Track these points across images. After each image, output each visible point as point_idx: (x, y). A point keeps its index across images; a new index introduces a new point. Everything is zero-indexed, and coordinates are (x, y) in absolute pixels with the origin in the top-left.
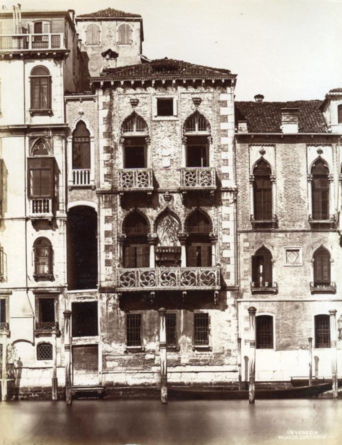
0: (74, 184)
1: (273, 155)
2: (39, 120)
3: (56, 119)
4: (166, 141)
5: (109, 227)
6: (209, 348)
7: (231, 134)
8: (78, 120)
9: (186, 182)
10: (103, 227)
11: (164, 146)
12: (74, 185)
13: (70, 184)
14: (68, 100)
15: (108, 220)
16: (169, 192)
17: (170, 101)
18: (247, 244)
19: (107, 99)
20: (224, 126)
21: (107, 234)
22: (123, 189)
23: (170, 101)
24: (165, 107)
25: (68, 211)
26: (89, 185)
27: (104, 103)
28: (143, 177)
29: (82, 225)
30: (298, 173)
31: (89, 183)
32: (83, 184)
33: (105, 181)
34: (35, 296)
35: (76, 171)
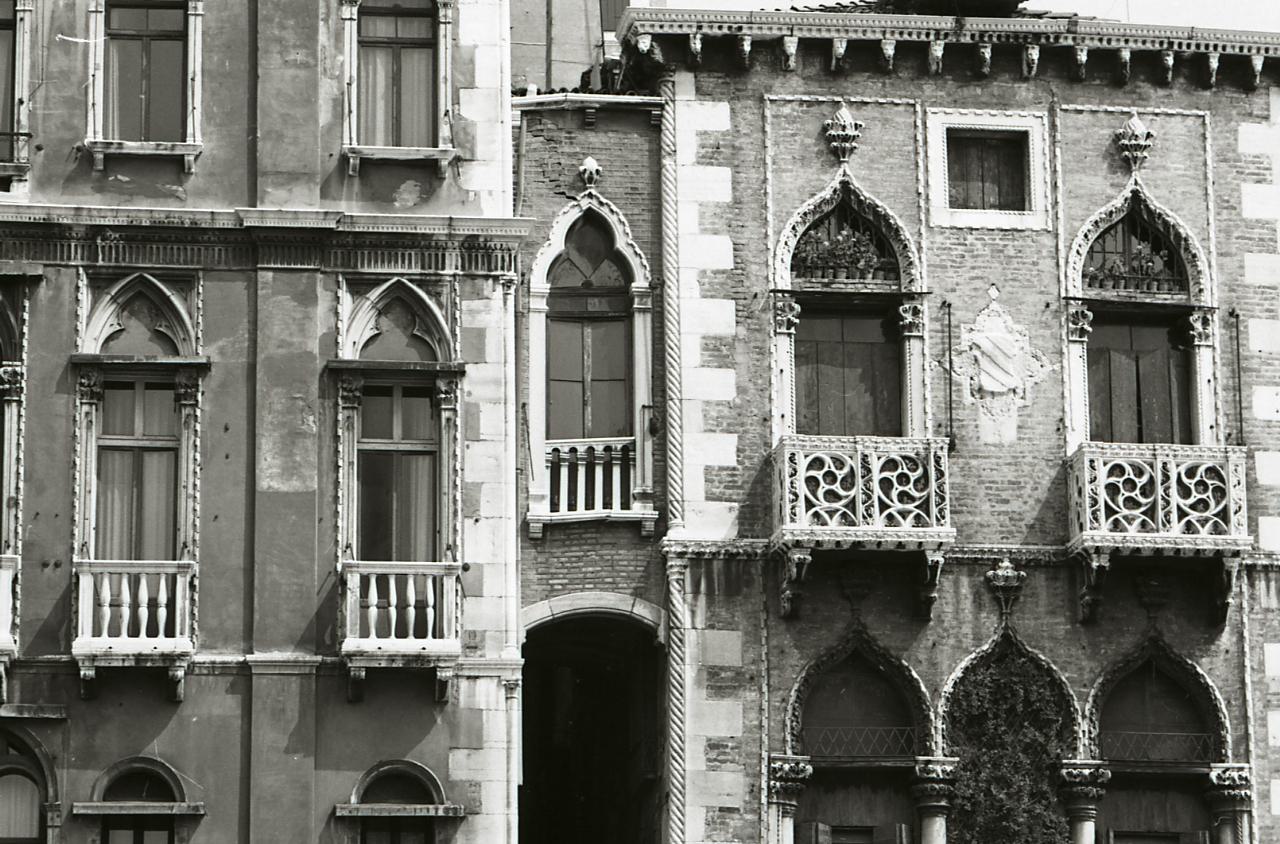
0: (555, 507)
9: (1110, 512)
10: (699, 719)
11: (986, 346)
12: (556, 517)
15: (719, 682)
16: (1017, 565)
17: (1015, 145)
22: (812, 532)
23: (1015, 145)
24: (993, 166)
26: (626, 514)
28: (903, 479)
31: (625, 505)
32: (599, 512)
33: (708, 499)
35: (564, 446)
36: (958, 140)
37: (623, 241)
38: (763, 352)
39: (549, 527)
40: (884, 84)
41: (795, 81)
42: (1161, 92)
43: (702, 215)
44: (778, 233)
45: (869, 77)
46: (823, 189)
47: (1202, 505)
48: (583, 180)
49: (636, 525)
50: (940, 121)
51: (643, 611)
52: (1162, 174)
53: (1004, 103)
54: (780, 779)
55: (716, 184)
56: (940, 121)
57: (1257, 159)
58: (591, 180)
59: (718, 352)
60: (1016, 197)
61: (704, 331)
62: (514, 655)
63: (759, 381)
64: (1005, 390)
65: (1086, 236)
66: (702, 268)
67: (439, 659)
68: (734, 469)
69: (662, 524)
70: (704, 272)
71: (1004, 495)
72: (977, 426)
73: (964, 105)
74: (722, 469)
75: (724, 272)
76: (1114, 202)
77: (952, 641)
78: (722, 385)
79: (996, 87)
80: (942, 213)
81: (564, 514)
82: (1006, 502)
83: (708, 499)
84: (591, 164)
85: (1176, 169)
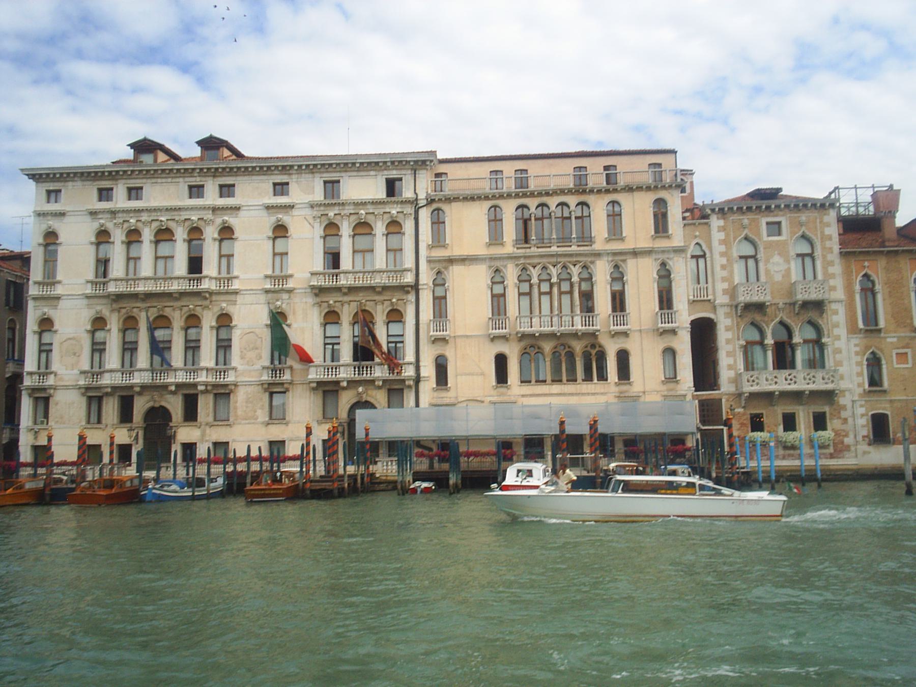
1: (879, 270)
2: (662, 244)
4: (776, 259)
5: (729, 335)
13: (691, 297)
15: (728, 329)
18: (858, 349)
19: (721, 223)
20: (828, 244)
21: (728, 341)
29: (703, 334)
36: (768, 223)
37: (704, 247)
38: (732, 267)
48: (696, 237)
49: (709, 300)
50: (764, 221)
51: (712, 316)
55: (722, 236)
59: (723, 267)
60: (780, 234)
69: (715, 300)
78: (724, 273)
79: (775, 213)
80: (765, 238)
84: (697, 233)
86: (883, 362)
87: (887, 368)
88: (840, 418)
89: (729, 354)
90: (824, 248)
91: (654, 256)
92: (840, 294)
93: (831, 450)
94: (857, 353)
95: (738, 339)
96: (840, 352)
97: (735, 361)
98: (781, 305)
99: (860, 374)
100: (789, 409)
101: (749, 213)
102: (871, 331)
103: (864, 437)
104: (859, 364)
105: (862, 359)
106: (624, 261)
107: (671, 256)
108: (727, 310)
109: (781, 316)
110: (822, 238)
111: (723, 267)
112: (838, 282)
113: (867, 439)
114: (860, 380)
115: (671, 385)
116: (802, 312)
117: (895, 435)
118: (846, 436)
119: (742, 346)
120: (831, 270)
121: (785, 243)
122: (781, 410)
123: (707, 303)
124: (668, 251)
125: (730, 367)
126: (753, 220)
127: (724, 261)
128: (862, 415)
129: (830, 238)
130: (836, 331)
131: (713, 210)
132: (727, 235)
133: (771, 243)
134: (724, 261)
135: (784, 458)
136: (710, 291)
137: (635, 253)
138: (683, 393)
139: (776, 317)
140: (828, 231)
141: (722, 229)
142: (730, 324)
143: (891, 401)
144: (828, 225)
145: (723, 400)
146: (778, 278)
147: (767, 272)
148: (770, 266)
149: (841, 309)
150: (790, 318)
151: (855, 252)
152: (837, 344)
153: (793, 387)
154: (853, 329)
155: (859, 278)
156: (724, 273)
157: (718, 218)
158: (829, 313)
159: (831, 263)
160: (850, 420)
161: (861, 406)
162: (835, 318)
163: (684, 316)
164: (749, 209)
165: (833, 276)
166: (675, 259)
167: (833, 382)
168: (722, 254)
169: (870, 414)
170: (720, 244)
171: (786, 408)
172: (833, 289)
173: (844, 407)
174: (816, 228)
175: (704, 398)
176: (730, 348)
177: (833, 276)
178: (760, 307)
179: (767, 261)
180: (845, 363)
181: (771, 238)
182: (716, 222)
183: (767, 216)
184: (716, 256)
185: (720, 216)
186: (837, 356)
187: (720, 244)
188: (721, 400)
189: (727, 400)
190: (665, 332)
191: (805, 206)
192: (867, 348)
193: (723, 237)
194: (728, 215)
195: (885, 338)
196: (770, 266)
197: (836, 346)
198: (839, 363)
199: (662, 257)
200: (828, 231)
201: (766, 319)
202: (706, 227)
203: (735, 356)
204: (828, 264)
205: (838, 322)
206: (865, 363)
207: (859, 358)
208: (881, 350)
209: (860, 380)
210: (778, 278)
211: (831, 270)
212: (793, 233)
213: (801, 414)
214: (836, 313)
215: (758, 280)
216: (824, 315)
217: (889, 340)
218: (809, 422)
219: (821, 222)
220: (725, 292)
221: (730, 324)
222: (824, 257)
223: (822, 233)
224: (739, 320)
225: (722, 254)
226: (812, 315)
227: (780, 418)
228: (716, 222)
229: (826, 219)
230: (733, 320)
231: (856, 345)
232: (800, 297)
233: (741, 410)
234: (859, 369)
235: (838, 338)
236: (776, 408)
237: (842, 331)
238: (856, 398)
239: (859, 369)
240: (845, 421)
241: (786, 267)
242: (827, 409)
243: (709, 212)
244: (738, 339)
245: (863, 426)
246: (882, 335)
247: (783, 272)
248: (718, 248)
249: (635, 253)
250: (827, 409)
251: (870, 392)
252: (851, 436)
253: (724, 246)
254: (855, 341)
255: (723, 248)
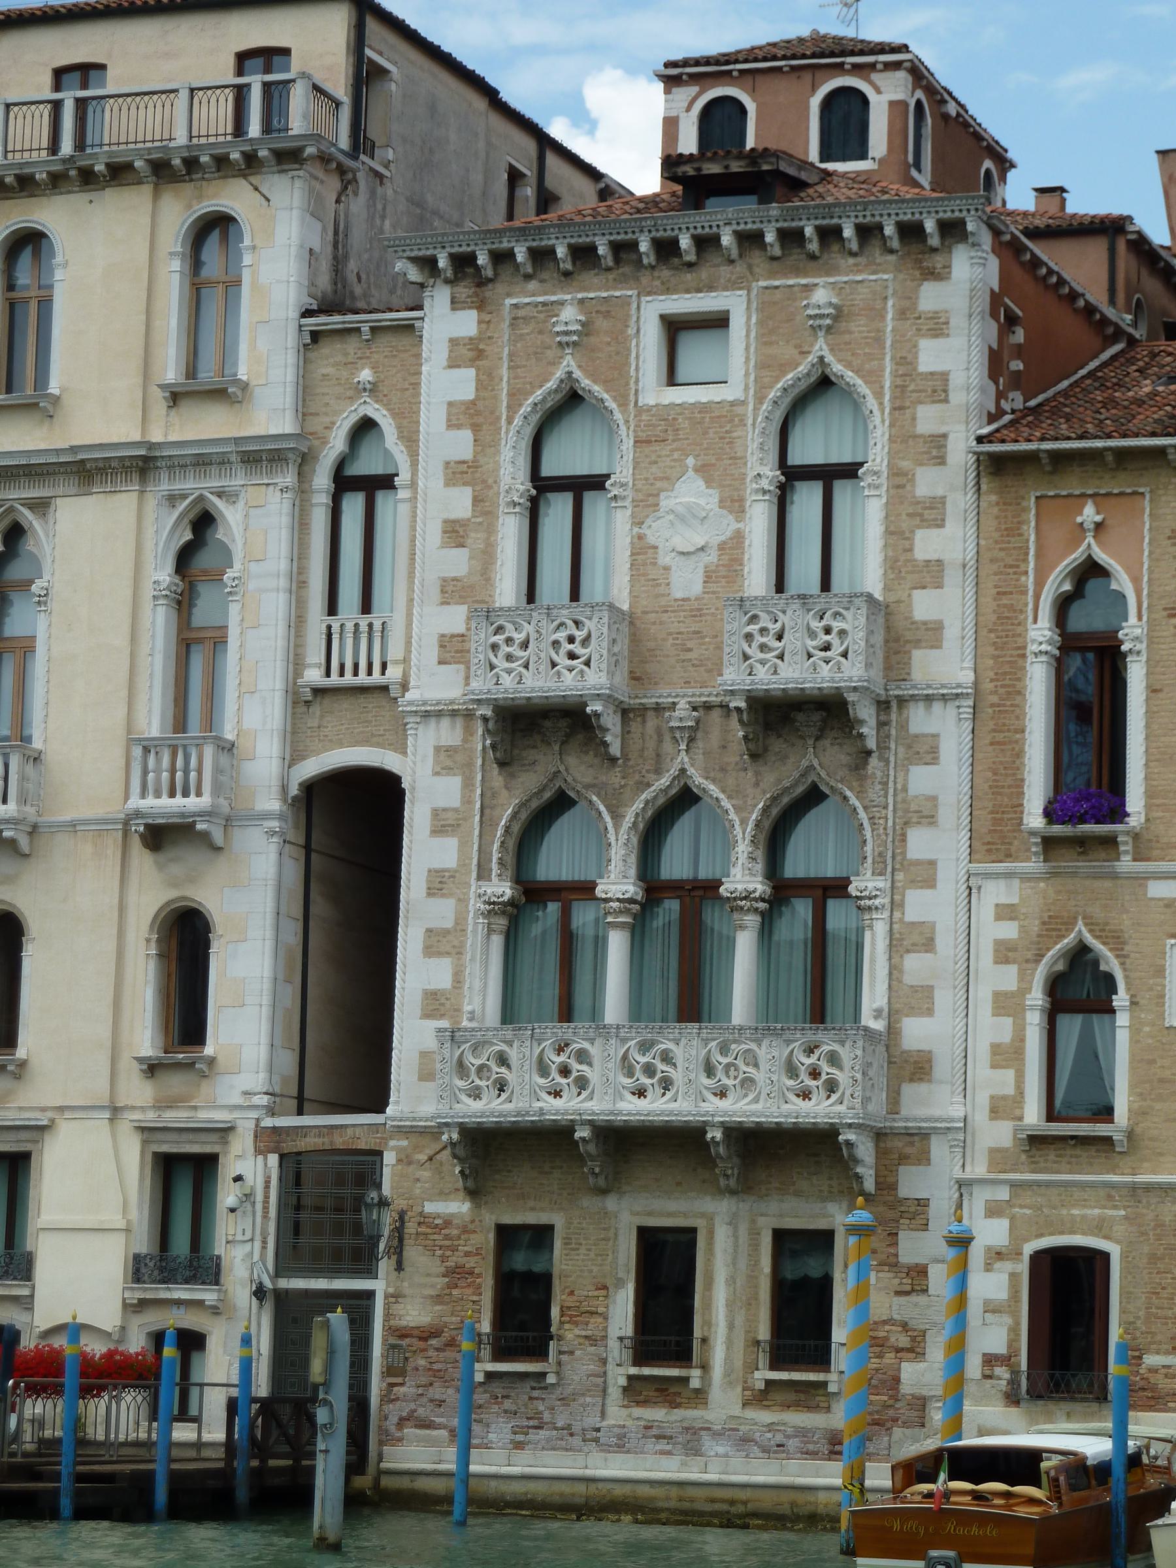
2: (207, 425)
3: (271, 415)
4: (691, 492)
6: (824, 1384)
7: (961, 448)
8: (354, 418)
10: (423, 852)
11: (680, 509)
13: (314, 676)
14: (316, 336)
15: (442, 825)
18: (1009, 931)
19: (467, 323)
20: (927, 419)
21: (439, 883)
25: (294, 790)
27: (454, 342)
30: (907, 535)
33: (440, 663)
34: (145, 1143)
39: (319, 692)
40: (607, 280)
41: (533, 285)
42: (851, 261)
43: (449, 414)
44: (510, 421)
45: (596, 275)
46: (548, 381)
47: (827, 648)
49: (384, 689)
50: (650, 312)
51: (389, 760)
52: (847, 337)
53: (711, 288)
54: (485, 902)
56: (650, 312)
57: (935, 316)
58: (365, 390)
61: (446, 516)
62: (274, 805)
63: (487, 558)
64: (692, 549)
65: (775, 402)
66: (448, 459)
67: (194, 815)
68: (463, 635)
69: (405, 686)
70: (448, 463)
71: (689, 645)
72: (668, 584)
73: (675, 291)
74: (453, 636)
75: (464, 462)
76: (800, 369)
77: (637, 777)
78: (458, 563)
79: (704, 273)
80: (653, 392)
81: (335, 680)
82: (690, 650)
83: (440, 663)
84: (366, 375)
85: (860, 332)
86: (1121, 999)
87: (1134, 1029)
88: (891, 1264)
89: (437, 943)
90: (902, 437)
91: (164, 485)
92: (950, 664)
93: (838, 1417)
94: (1004, 953)
95: (483, 874)
96: (928, 945)
97: (458, 979)
98: (682, 714)
99: (1007, 1055)
100: (669, 1209)
101: (590, 277)
102: (1082, 844)
103: (989, 1360)
104: (1006, 1004)
105: (1024, 978)
106: (41, 506)
107: (237, 479)
108: (448, 733)
109: (686, 764)
110: (900, 390)
111: (455, 532)
112: (949, 607)
113: (1002, 1372)
114: (1005, 1081)
115: (176, 1082)
116: (777, 745)
117: (1133, 1354)
118: (915, 1350)
119: (495, 908)
120: (927, 544)
121: (725, 418)
122: (631, 1211)
123: (371, 702)
124: (223, 462)
125: (435, 1004)
126: (607, 308)
127: (460, 503)
128: (996, 1255)
129: (938, 388)
130: (920, 843)
131: (429, 264)
132: (486, 383)
133: (668, 416)
134: (460, 503)
135: (621, 1445)
136: (395, 651)
137: (89, 470)
138: (220, 1116)
139: (658, 771)
140: (932, 356)
141: (466, 353)
142: (456, 802)
143: (1134, 1190)
144: (938, 327)
145: (389, 1158)
146: (687, 582)
147: (642, 551)
148: (658, 531)
149: (950, 729)
150: (718, 772)
151: (1031, 458)
152: (919, 905)
153: (655, 1108)
154: (993, 838)
155: (1057, 582)
156: (458, 563)
157: (455, 304)
158: (896, 751)
159: (932, 513)
160: (939, 1280)
161: (993, 1210)
162: (921, 780)
163: (264, 753)
164: (584, 255)
165: (932, 574)
166: (251, 495)
167: (831, 1087)
168: (459, 473)
169: (1029, 1248)
170: (452, 424)
171: (658, 1204)
172: (933, 633)
173: (917, 1213)
174: (879, 341)
175: (303, 1144)
176: (442, 912)
177: (932, 574)
178: (567, 722)
179: (646, 504)
180: (945, 999)
181: (675, 395)
182: (445, 320)
183: (668, 291)
184: (431, 480)
185: (464, 290)
186: (915, 965)
187: (452, 424)
188: (380, 1154)
189: (405, 1160)
190: (160, 836)
191: (830, 235)
192: (1054, 925)
193: (467, 392)
194: (500, 288)
195: (1142, 879)
196: (658, 531)
197: (911, 915)
198: (919, 1000)
199: (192, 485)
200: (932, 356)
201: (614, 778)
202: (404, 341)
203: (458, 952)
204: (912, 514)
205: (933, 799)
206: (1037, 997)
207: (1008, 978)
208: (1117, 942)
209: (1005, 1081)
210: (687, 582)
211: (927, 544)
212: (767, 367)
213: (722, 1235)
214: (929, 752)
215: (575, 595)
216: (874, 761)
217: (1158, 890)
218: (752, 1279)
219: (902, 314)
220: (452, 649)
221: (456, 802)
222: (900, 480)
223: (906, 362)
224: (497, 779)
225: (459, 473)
226: (824, 760)
227: (627, 1250)
228: (445, 320)
229: (931, 297)
230: (468, 785)
231: (1005, 912)
232: (745, 673)
233: (458, 1207)
234: (1004, 1029)
235: (926, 874)
236: (611, 1203)
237: (944, 843)
238: (979, 1169)
239: (1004, 1029)
240: (915, 1279)
241: (727, 525)
242: (841, 1218)
243: (414, 274)
244: (483, 874)
245: (991, 1308)
246: (1126, 864)
247: (712, 557)
248: (443, 443)
249: (89, 470)
250: (841, 1218)
251: (1036, 1141)
252: (936, 1353)
253: (465, 436)
254: (995, 893)
255: (462, 444)
